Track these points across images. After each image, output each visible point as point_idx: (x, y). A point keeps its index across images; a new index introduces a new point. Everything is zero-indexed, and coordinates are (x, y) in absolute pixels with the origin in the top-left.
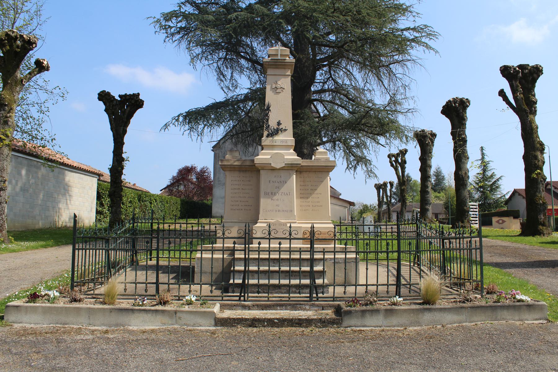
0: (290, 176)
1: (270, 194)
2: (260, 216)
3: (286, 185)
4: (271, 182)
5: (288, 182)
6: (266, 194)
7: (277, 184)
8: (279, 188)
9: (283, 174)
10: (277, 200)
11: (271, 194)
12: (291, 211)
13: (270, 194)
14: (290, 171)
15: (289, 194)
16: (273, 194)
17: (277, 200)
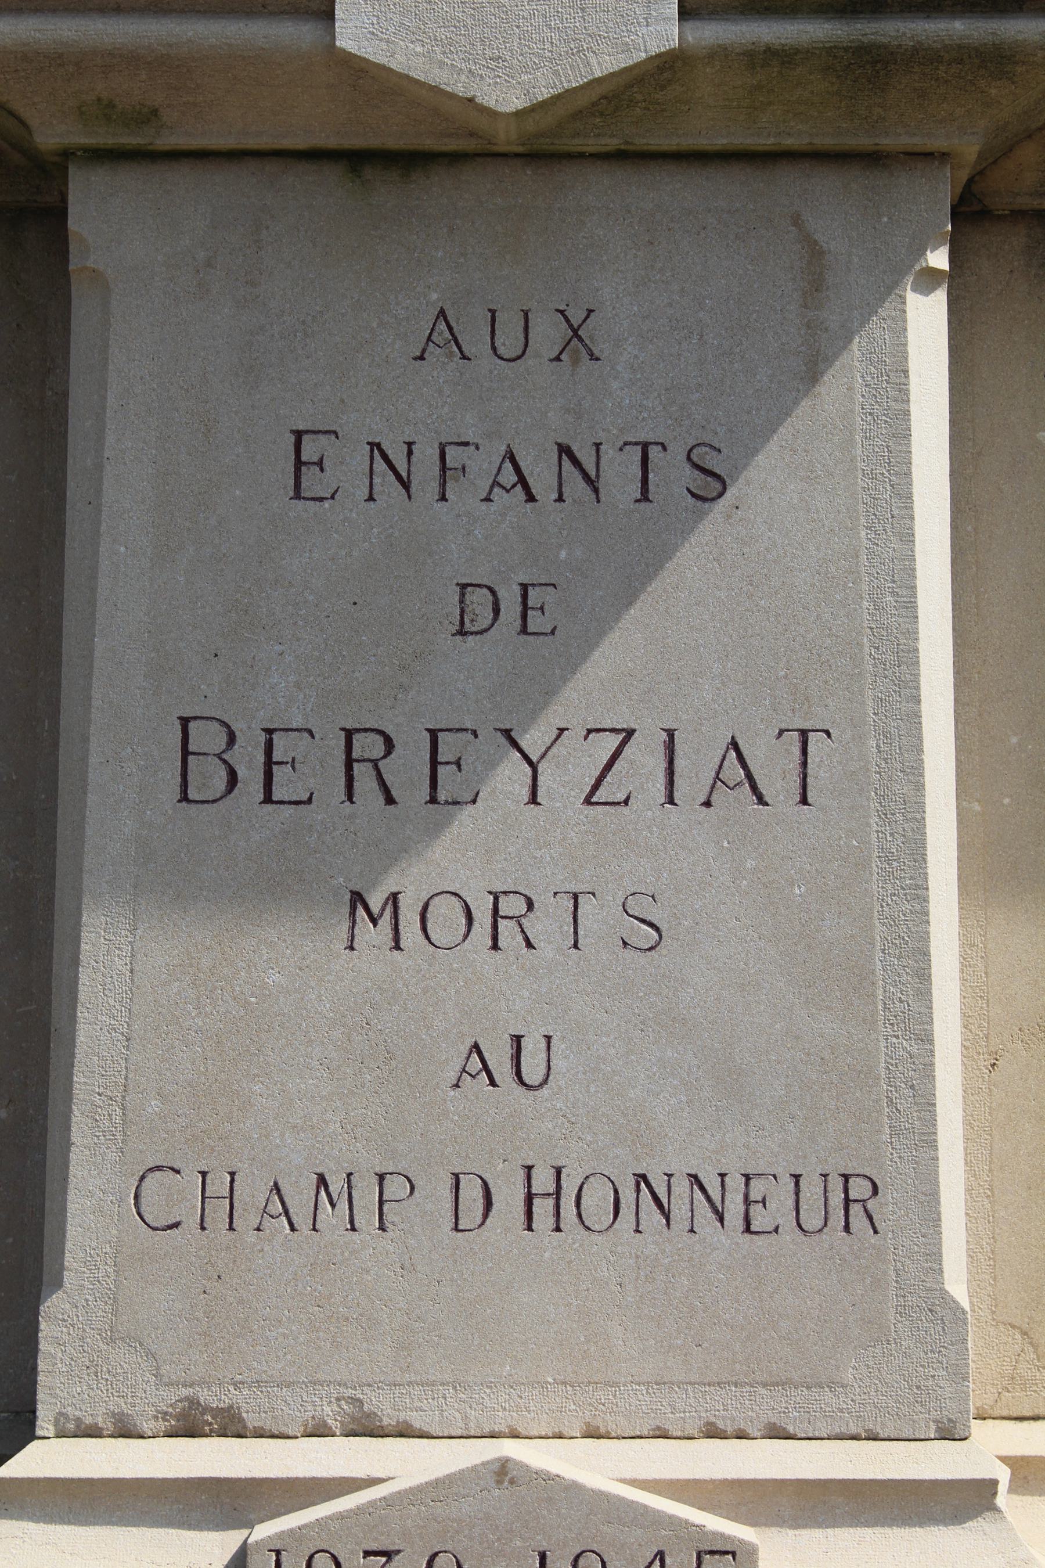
0: (818, 324)
1: (312, 770)
2: (66, 1332)
3: (703, 559)
4: (346, 468)
5: (766, 481)
6: (222, 765)
7: (479, 534)
8: (530, 620)
9: (642, 269)
10: (501, 918)
11: (339, 794)
12: (855, 1200)
13: (312, 770)
14: (829, 208)
15: (790, 762)
16: (406, 771)
17: (501, 918)
